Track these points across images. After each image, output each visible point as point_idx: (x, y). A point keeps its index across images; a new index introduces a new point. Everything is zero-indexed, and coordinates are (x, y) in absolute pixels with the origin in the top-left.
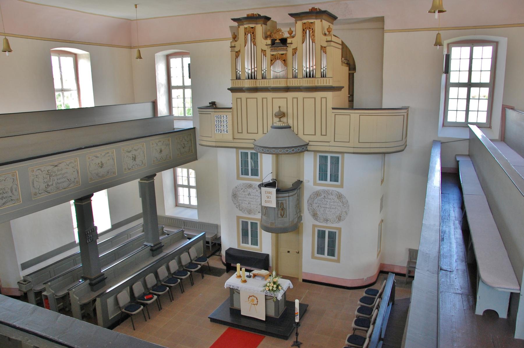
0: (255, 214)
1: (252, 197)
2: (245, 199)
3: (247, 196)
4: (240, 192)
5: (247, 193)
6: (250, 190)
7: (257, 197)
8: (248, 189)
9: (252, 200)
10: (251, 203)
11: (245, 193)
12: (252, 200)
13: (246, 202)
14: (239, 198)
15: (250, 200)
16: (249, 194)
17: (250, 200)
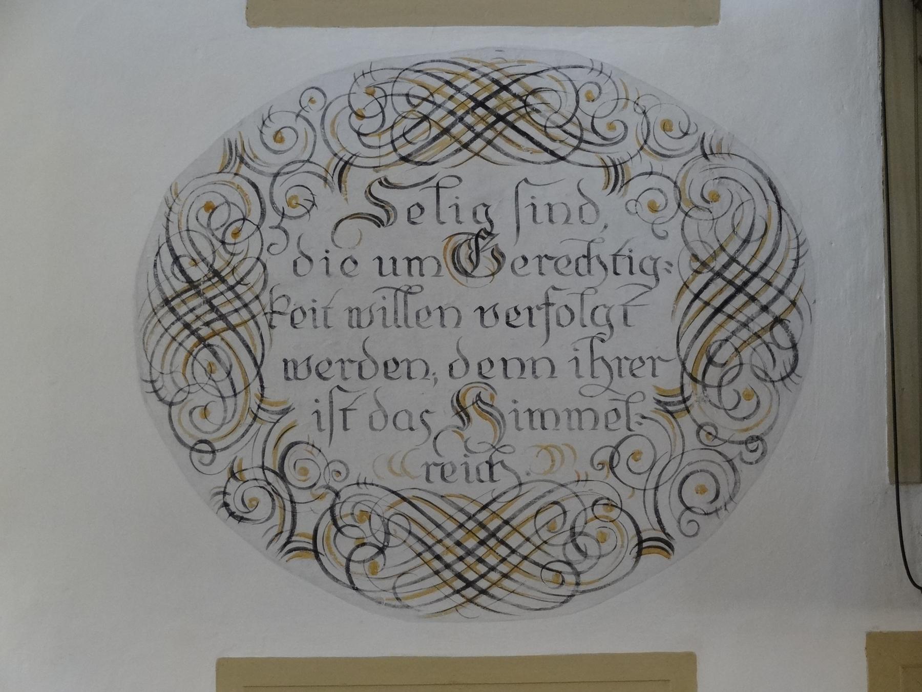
0: (569, 584)
1: (517, 289)
2: (388, 343)
3: (441, 287)
4: (314, 232)
5: (429, 240)
6: (486, 180)
7: (614, 292)
8: (446, 162)
9: (525, 342)
10: (507, 393)
11: (398, 240)
12: (525, 342)
13: (400, 394)
14: (285, 342)
15: (497, 341)
16: (474, 251)
17: (497, 341)
